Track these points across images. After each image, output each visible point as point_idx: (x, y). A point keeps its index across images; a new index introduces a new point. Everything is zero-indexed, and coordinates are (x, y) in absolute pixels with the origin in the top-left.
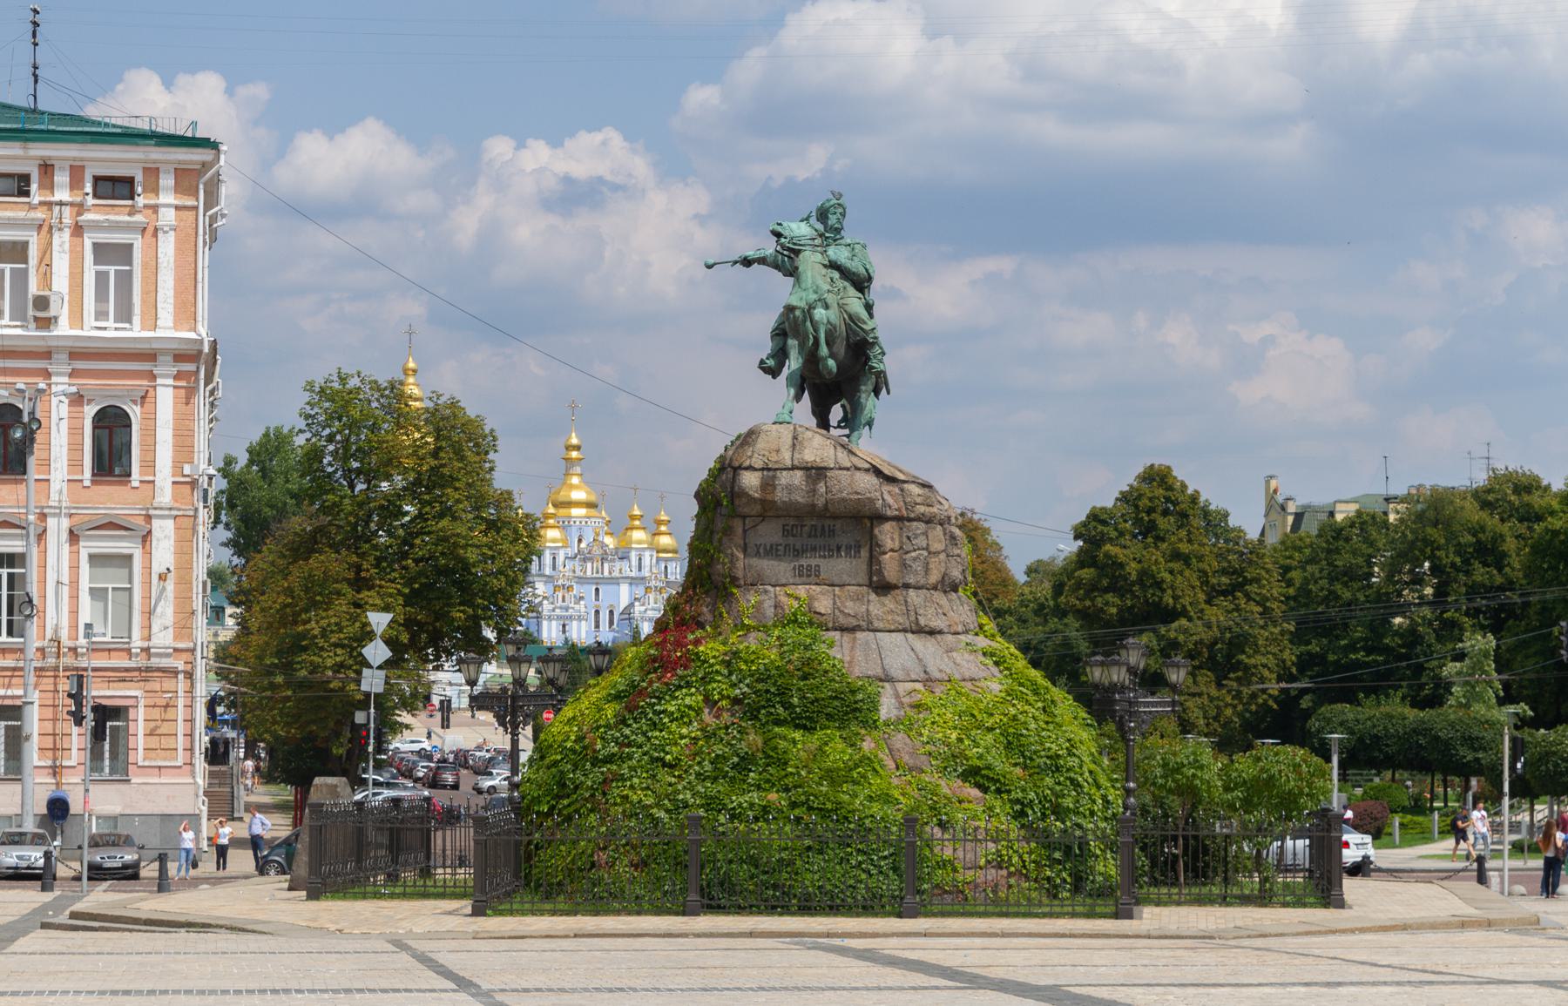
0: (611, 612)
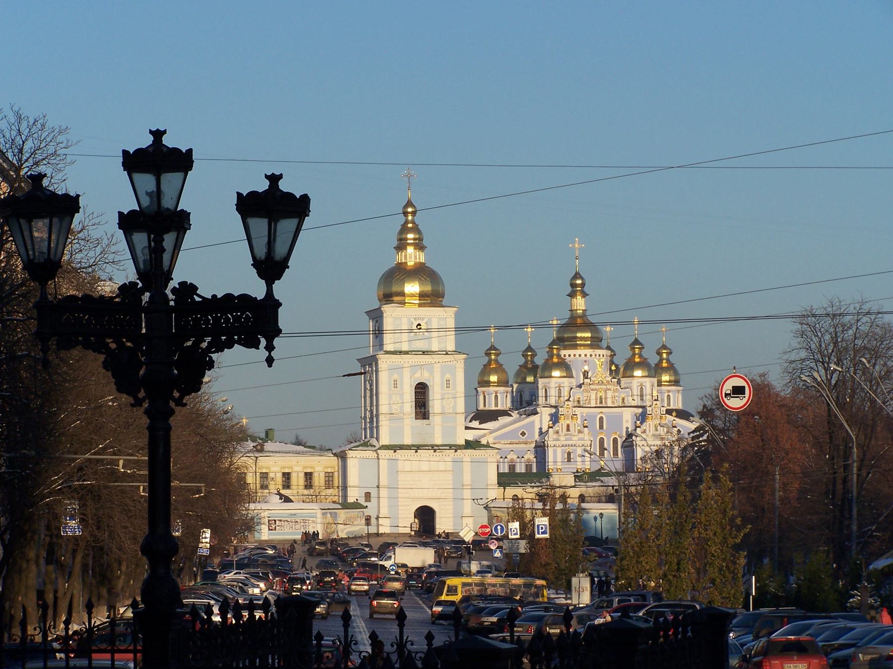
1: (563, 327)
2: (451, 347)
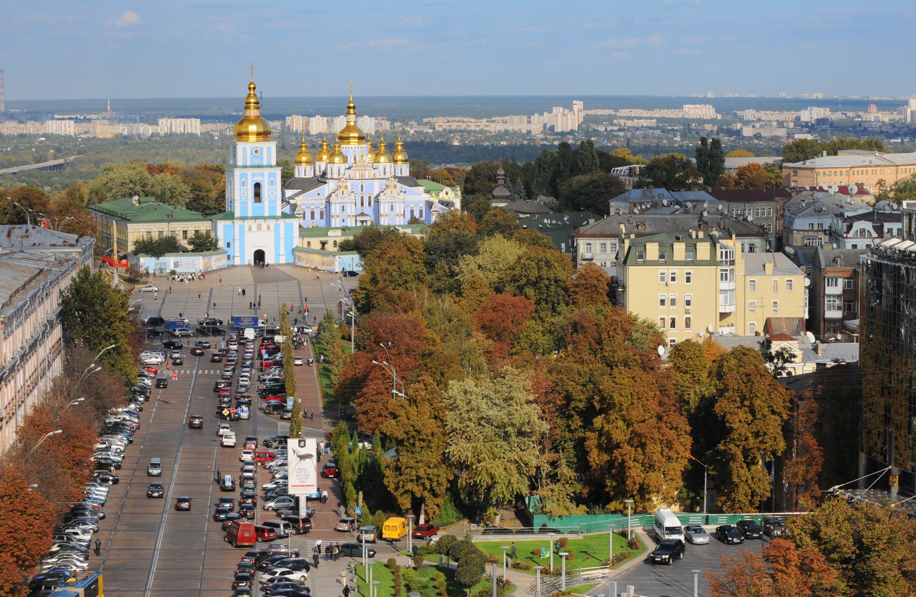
0: (370, 198)
1: (342, 132)
2: (274, 163)
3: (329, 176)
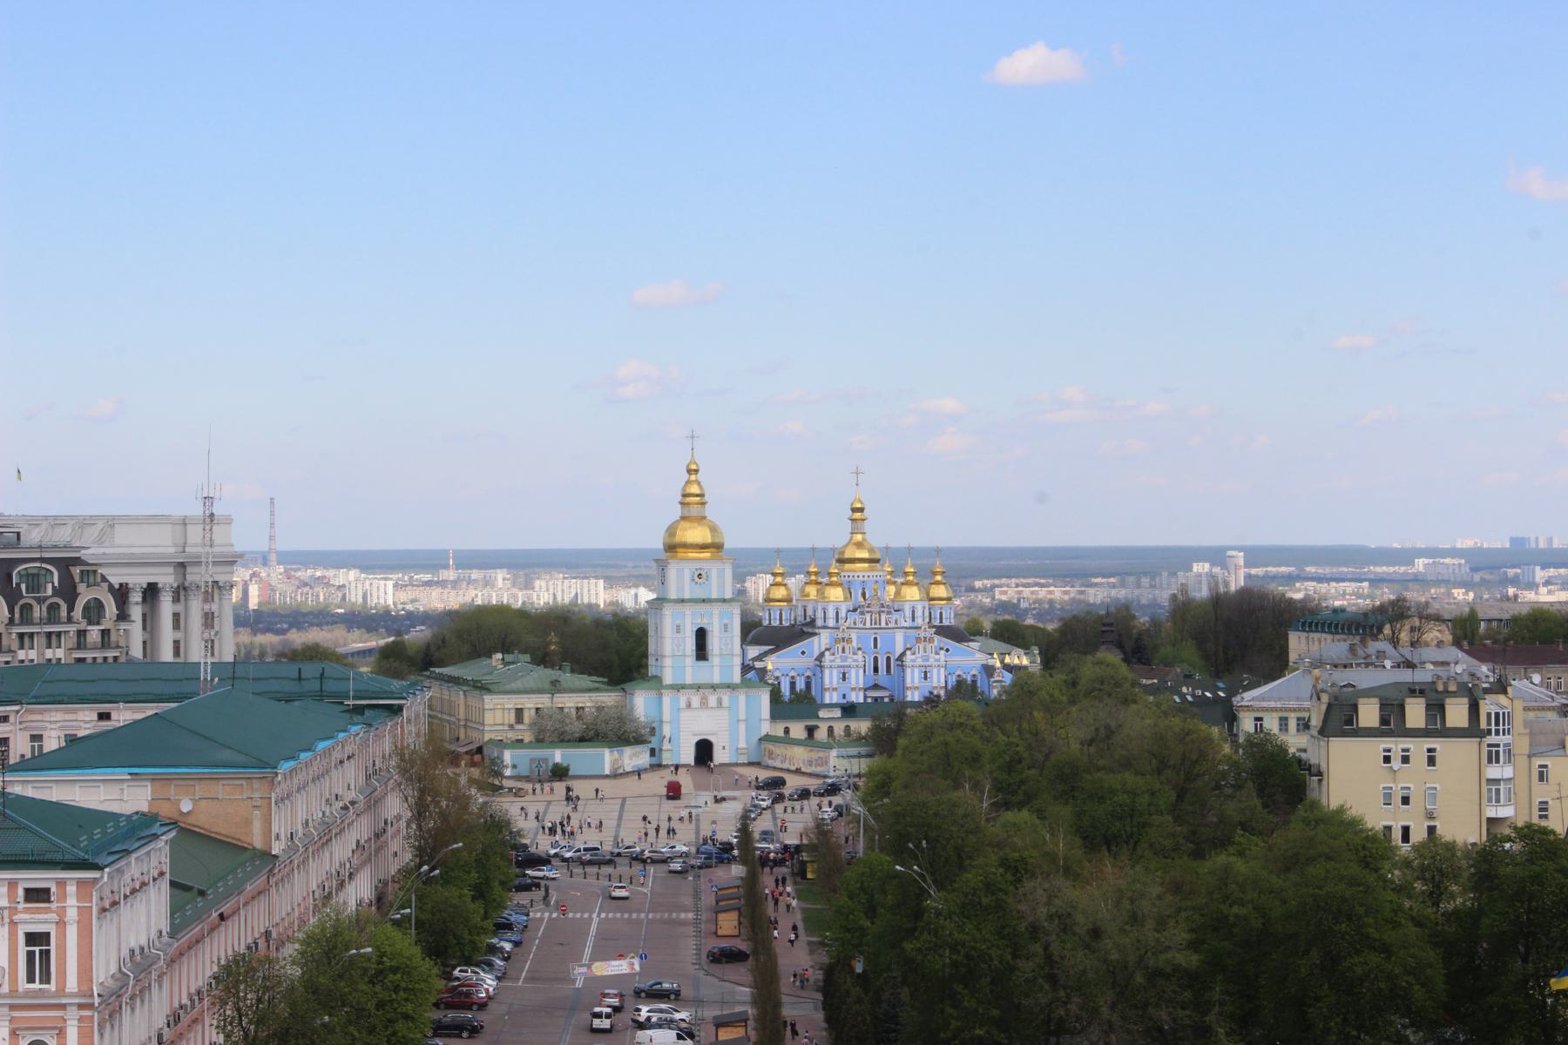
0: (888, 659)
3: (819, 622)
